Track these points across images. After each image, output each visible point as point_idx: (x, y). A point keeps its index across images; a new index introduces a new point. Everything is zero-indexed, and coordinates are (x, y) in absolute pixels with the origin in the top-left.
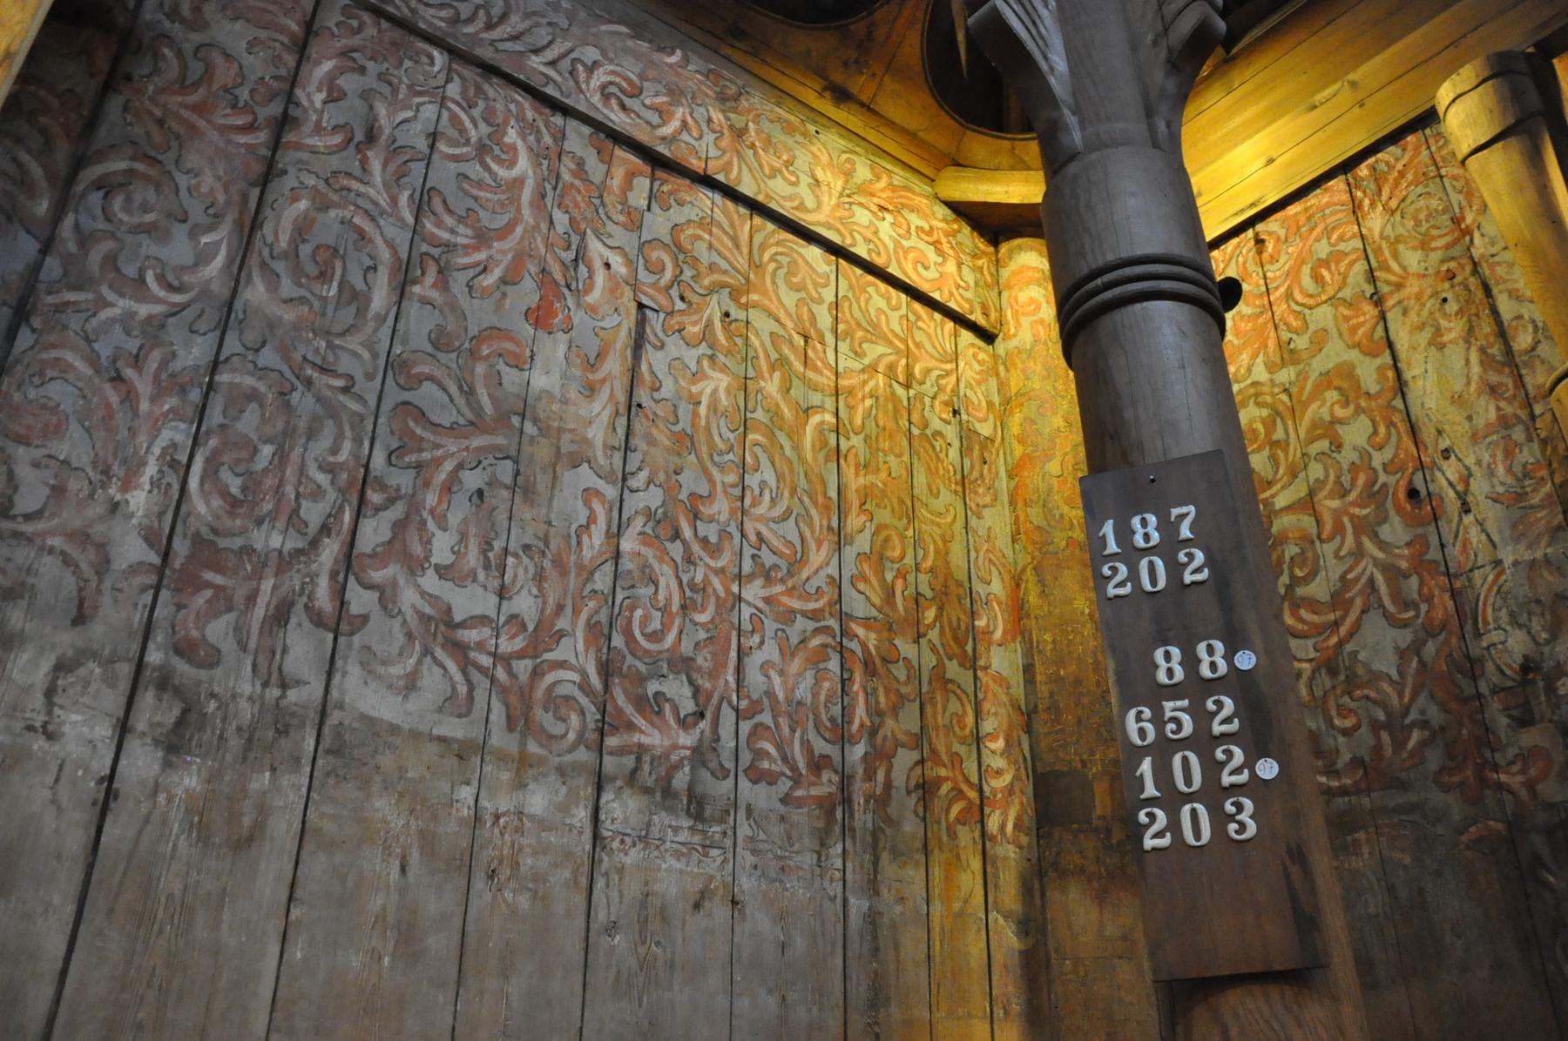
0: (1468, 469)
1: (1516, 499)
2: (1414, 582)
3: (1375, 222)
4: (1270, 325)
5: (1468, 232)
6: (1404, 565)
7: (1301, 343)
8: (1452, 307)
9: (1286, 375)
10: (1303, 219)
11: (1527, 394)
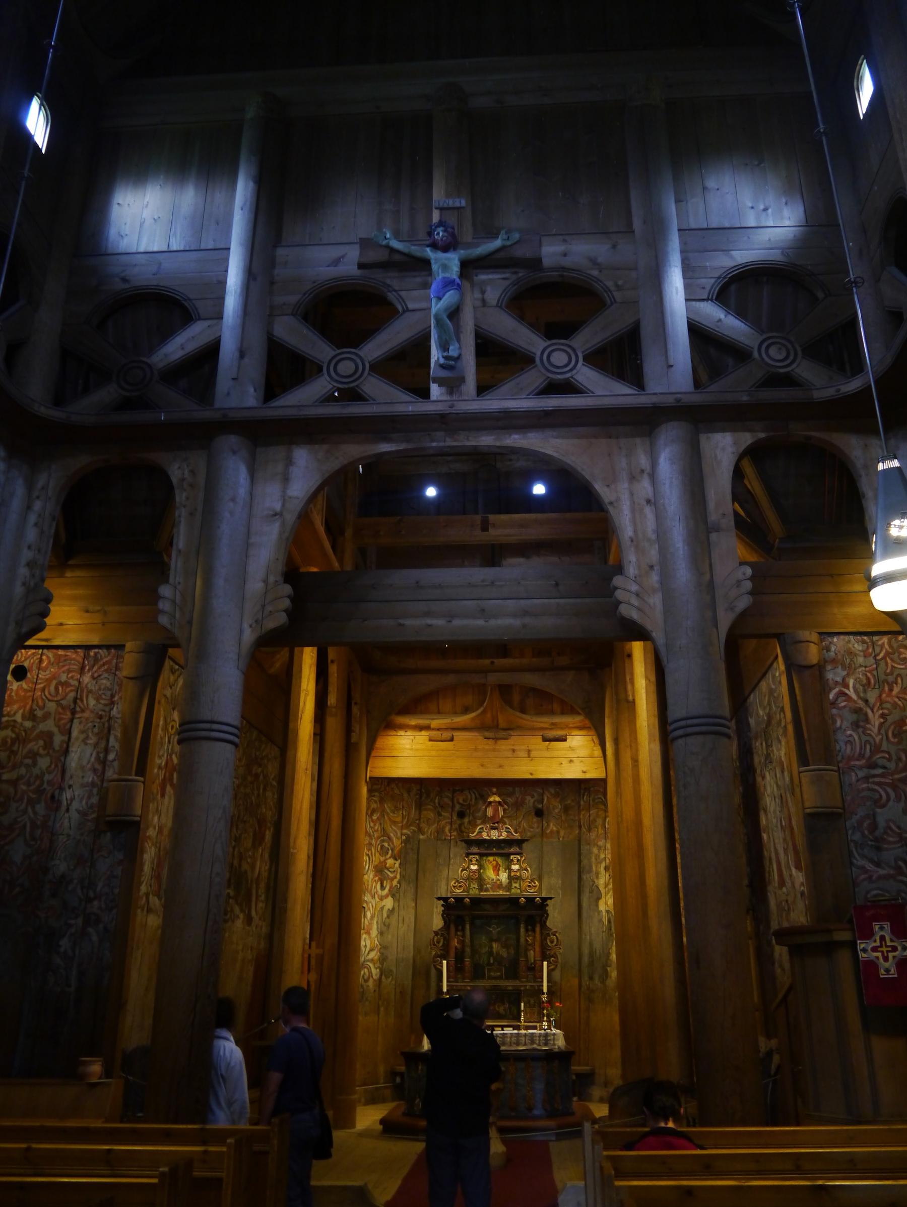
0: (74, 796)
1: (83, 814)
2: (39, 832)
3: (86, 679)
4: (31, 698)
5: (113, 703)
6: (39, 823)
7: (39, 713)
8: (96, 730)
9: (28, 724)
10: (63, 659)
11: (104, 778)
